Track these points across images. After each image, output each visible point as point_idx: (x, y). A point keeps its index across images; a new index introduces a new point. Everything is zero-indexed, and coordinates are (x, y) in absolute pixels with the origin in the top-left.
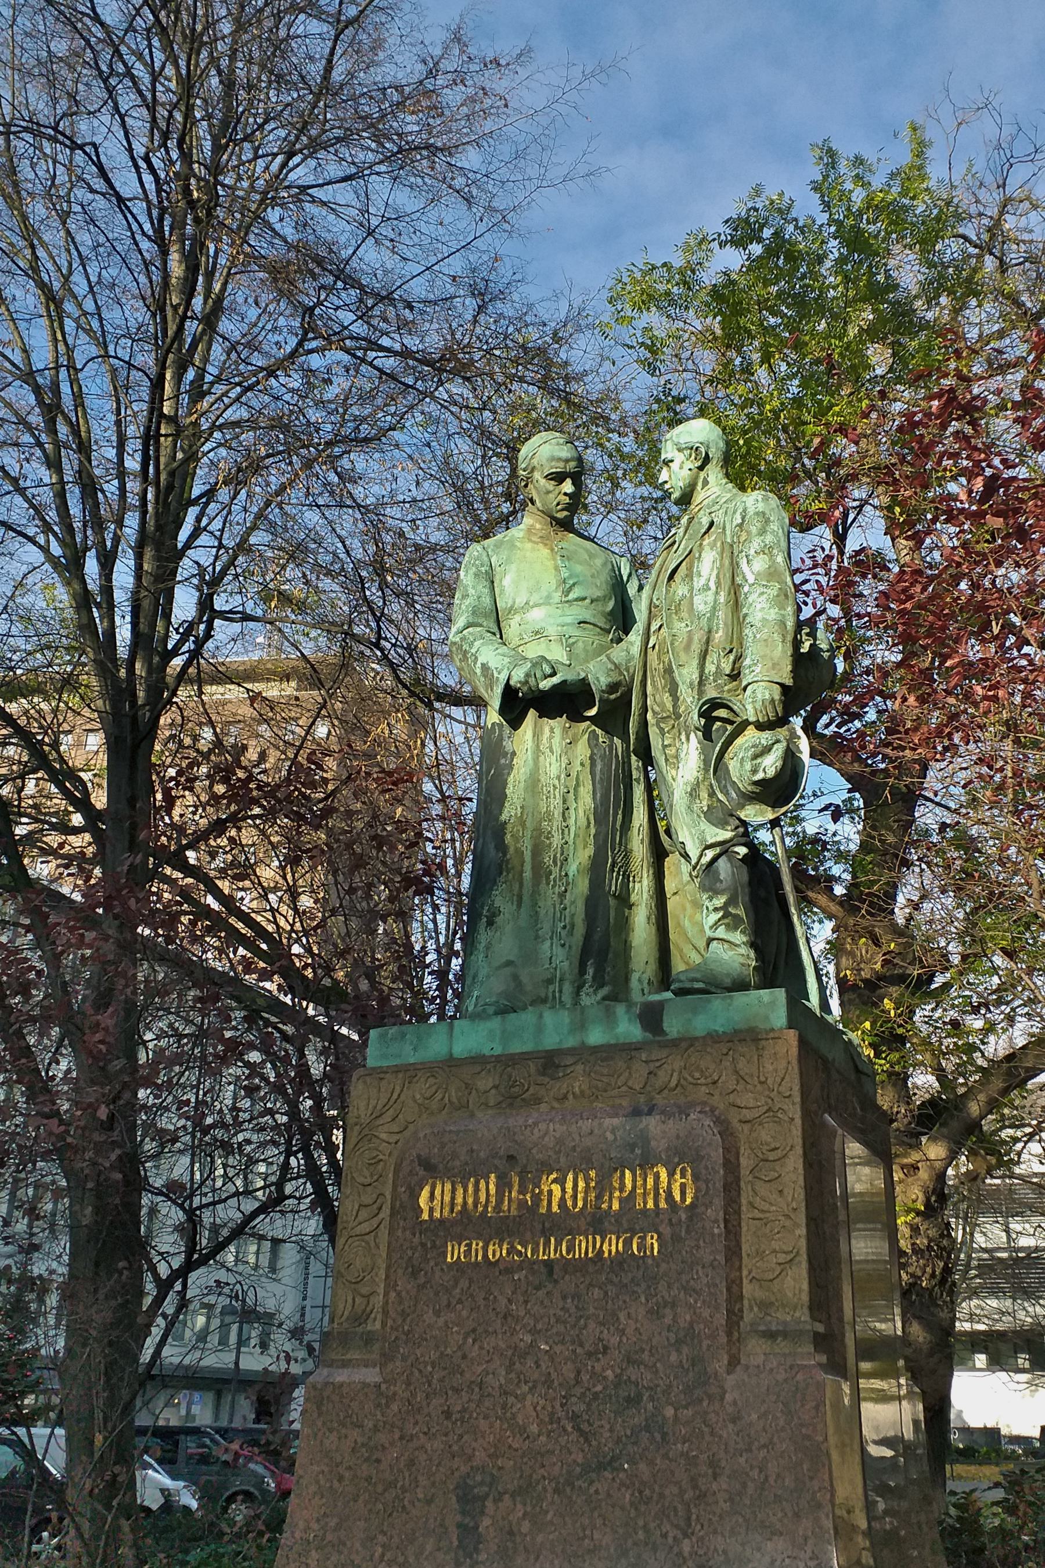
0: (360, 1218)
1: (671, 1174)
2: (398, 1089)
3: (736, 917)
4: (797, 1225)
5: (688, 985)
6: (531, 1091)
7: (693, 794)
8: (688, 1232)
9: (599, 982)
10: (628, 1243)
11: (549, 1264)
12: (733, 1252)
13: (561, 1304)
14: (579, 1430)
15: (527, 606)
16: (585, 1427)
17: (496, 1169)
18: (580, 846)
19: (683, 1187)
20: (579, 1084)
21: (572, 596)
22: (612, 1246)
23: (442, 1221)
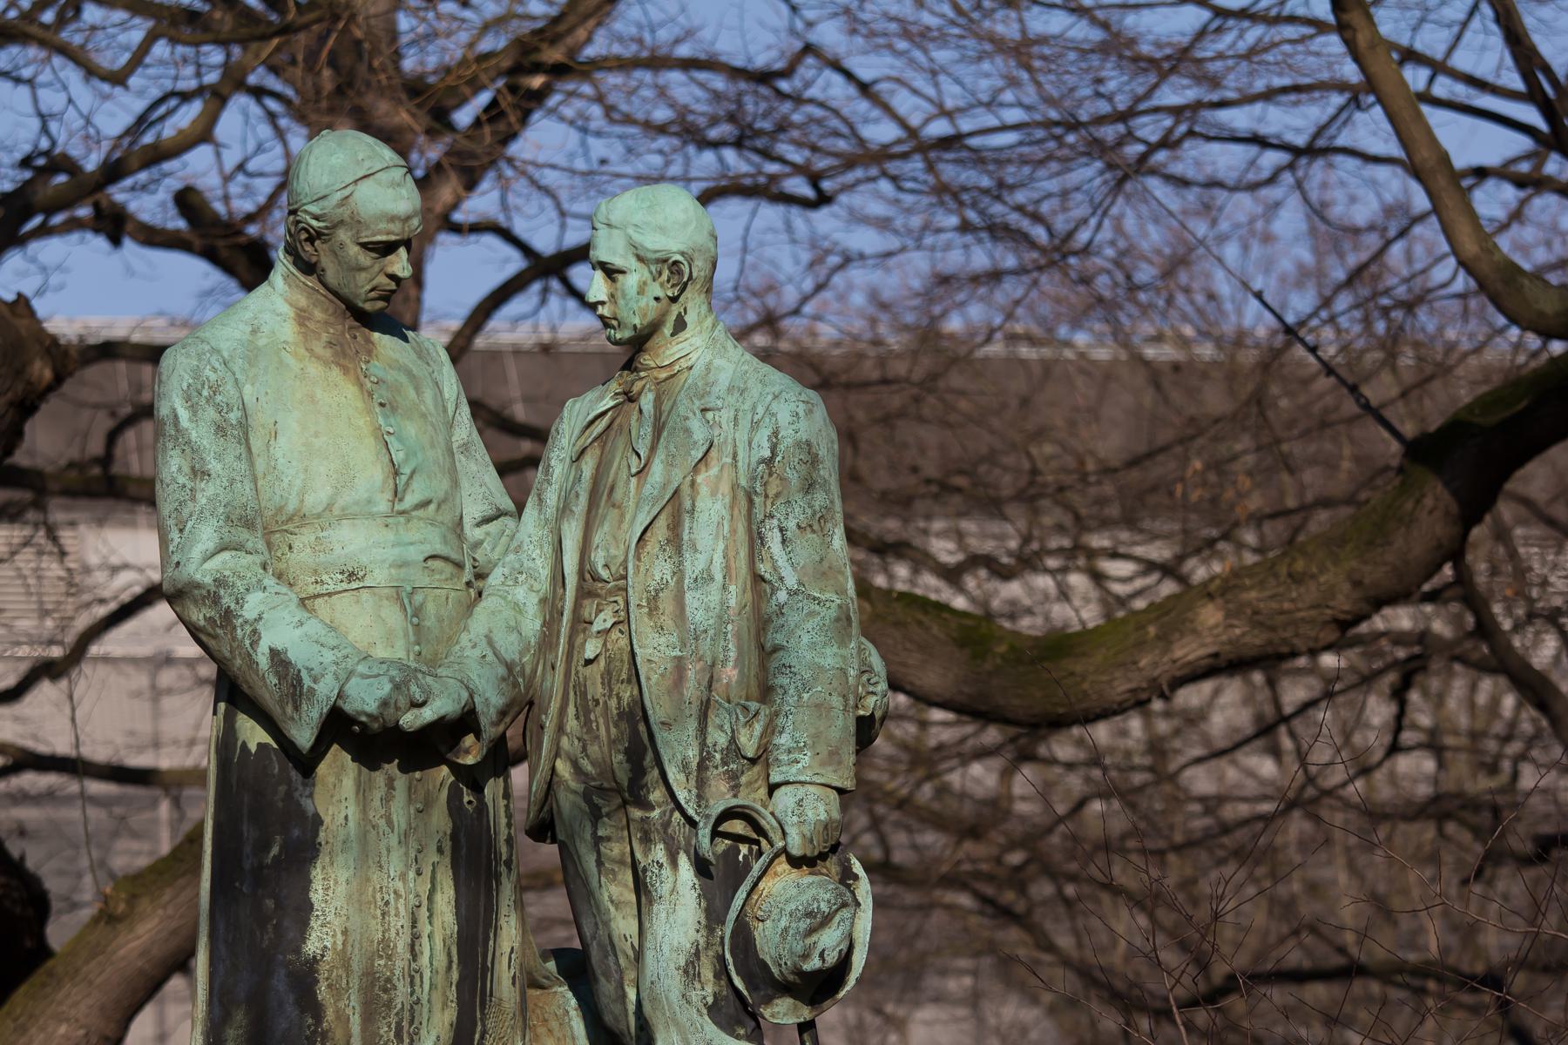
7: (690, 971)
15: (330, 515)
18: (437, 1006)
21: (410, 500)
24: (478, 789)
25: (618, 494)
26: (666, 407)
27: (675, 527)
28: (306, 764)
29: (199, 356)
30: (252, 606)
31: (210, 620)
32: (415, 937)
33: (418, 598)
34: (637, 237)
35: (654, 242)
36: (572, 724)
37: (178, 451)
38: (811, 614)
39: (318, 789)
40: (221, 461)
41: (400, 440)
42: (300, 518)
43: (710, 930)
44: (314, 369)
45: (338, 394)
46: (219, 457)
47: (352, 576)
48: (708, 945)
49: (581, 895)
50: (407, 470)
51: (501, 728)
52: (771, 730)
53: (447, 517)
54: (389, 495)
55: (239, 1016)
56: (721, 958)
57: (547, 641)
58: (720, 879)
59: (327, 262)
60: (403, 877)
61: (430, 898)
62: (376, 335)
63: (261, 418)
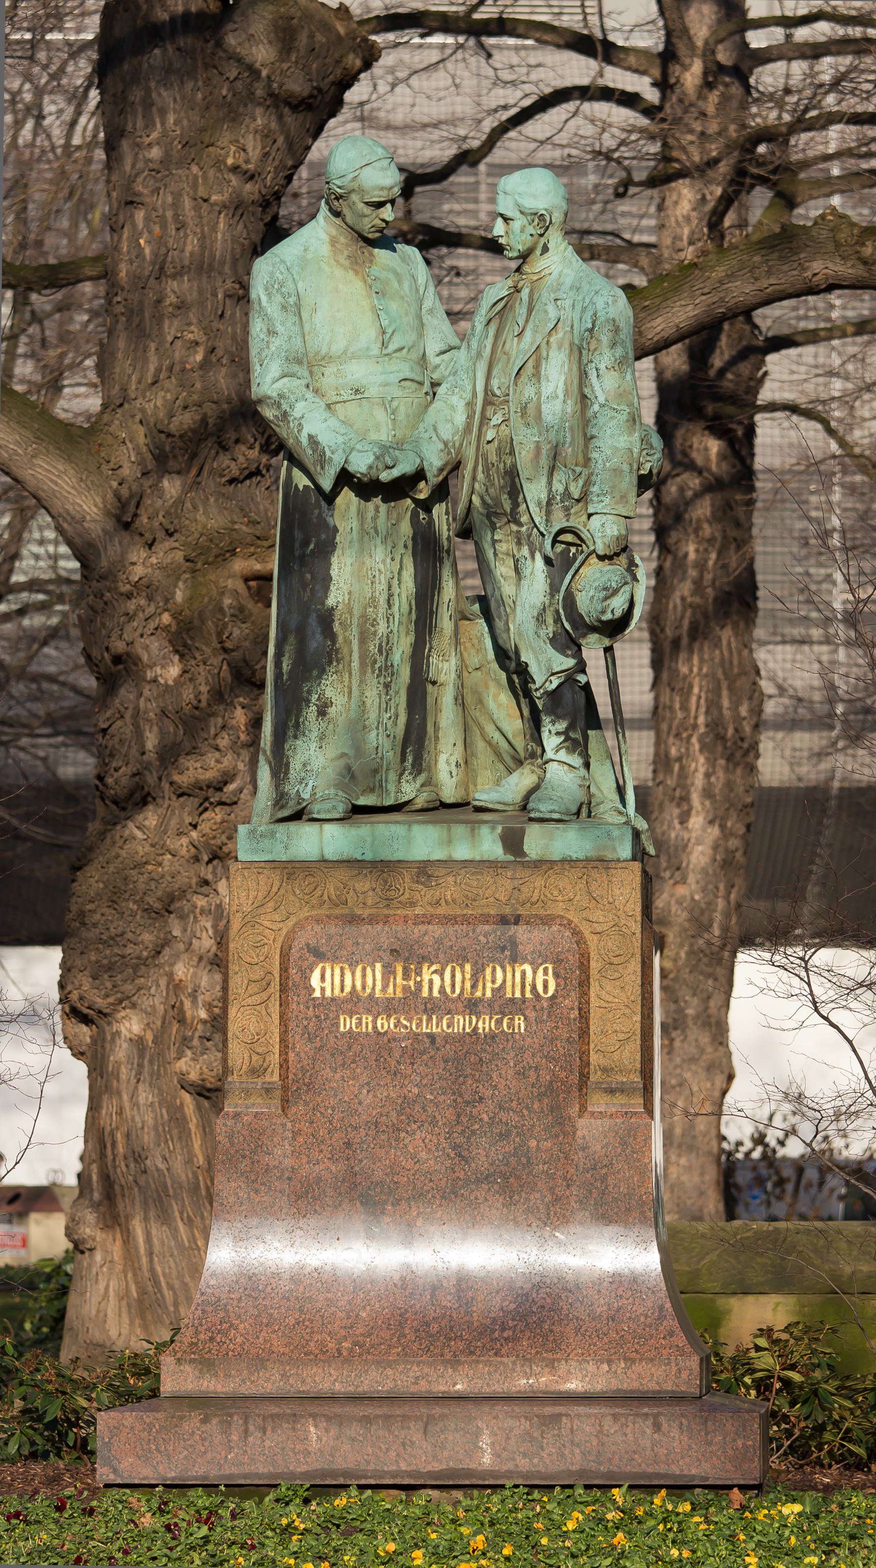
1: (535, 972)
3: (575, 742)
5: (548, 816)
6: (407, 895)
7: (540, 619)
8: (549, 1016)
10: (499, 1022)
11: (432, 1037)
12: (584, 1033)
13: (442, 1065)
14: (460, 1156)
15: (345, 356)
18: (403, 634)
21: (392, 347)
22: (485, 1024)
23: (333, 999)
24: (428, 511)
25: (507, 347)
26: (536, 297)
27: (537, 367)
28: (330, 498)
29: (274, 265)
30: (298, 410)
31: (276, 417)
32: (391, 596)
33: (395, 404)
34: (520, 201)
35: (530, 204)
36: (480, 476)
37: (259, 320)
38: (612, 418)
39: (336, 512)
40: (284, 325)
41: (387, 313)
42: (328, 359)
43: (552, 596)
44: (339, 272)
45: (352, 286)
46: (283, 323)
48: (551, 604)
49: (484, 570)
50: (390, 331)
51: (441, 478)
52: (588, 483)
53: (415, 355)
54: (379, 345)
55: (292, 639)
56: (557, 612)
57: (468, 428)
58: (560, 566)
59: (346, 211)
60: (384, 562)
61: (399, 574)
62: (376, 251)
63: (307, 301)
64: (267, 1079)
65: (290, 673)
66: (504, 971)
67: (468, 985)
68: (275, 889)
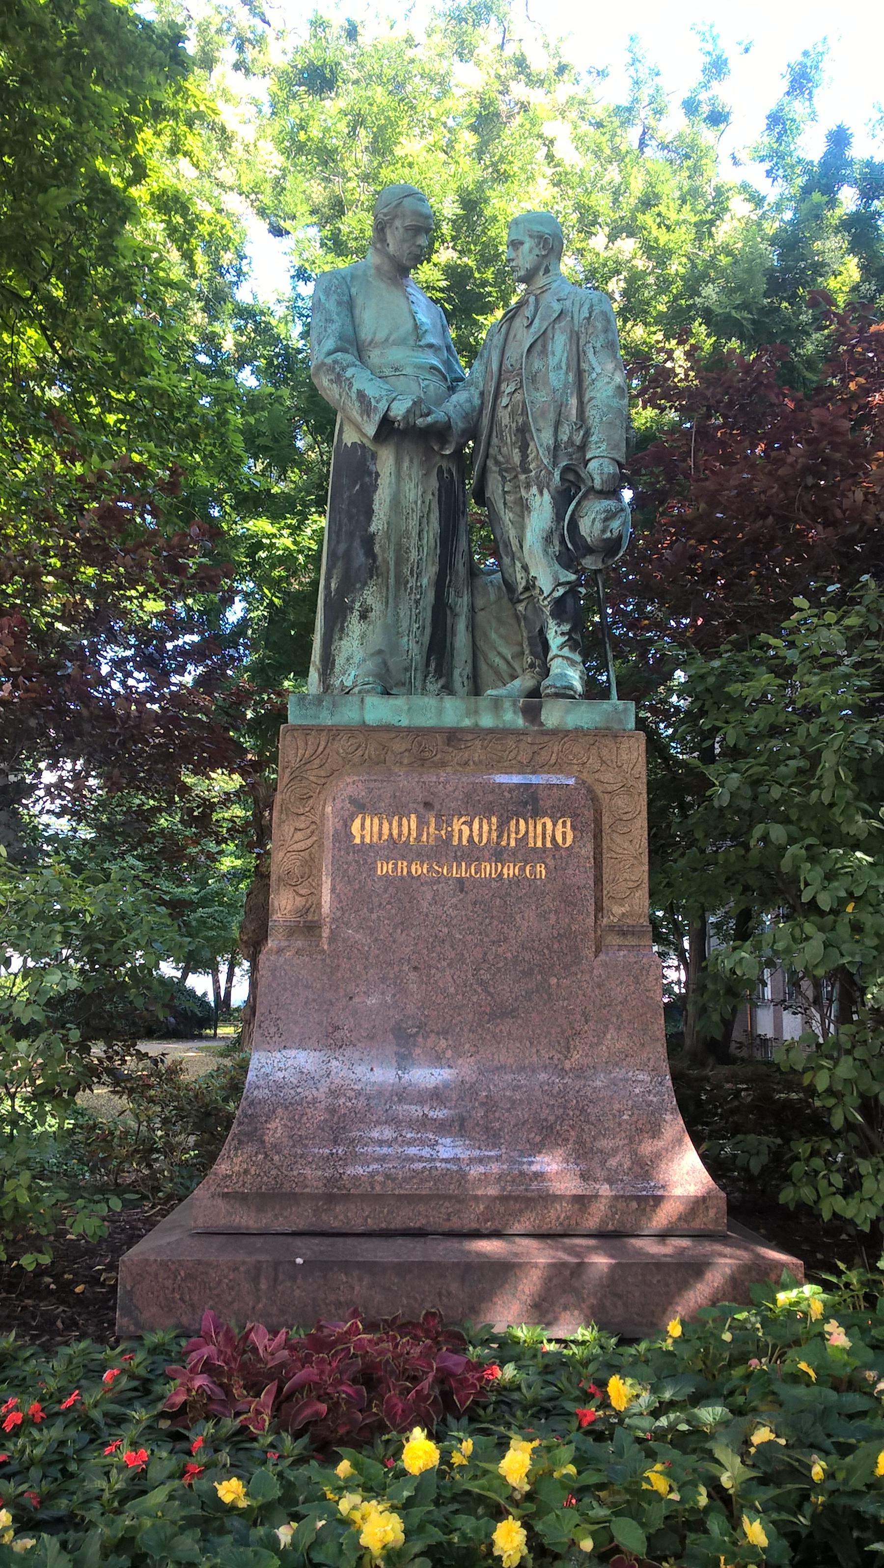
0: (296, 838)
1: (554, 825)
2: (323, 744)
3: (575, 641)
4: (642, 864)
7: (548, 540)
9: (439, 673)
10: (522, 869)
11: (461, 881)
12: (598, 881)
16: (492, 990)
17: (416, 812)
19: (564, 833)
20: (478, 754)
22: (510, 871)
23: (371, 846)
27: (544, 346)
36: (495, 441)
44: (383, 285)
47: (397, 369)
52: (587, 434)
55: (340, 564)
64: (310, 918)
65: (337, 590)
66: (527, 823)
67: (494, 835)
68: (321, 748)
